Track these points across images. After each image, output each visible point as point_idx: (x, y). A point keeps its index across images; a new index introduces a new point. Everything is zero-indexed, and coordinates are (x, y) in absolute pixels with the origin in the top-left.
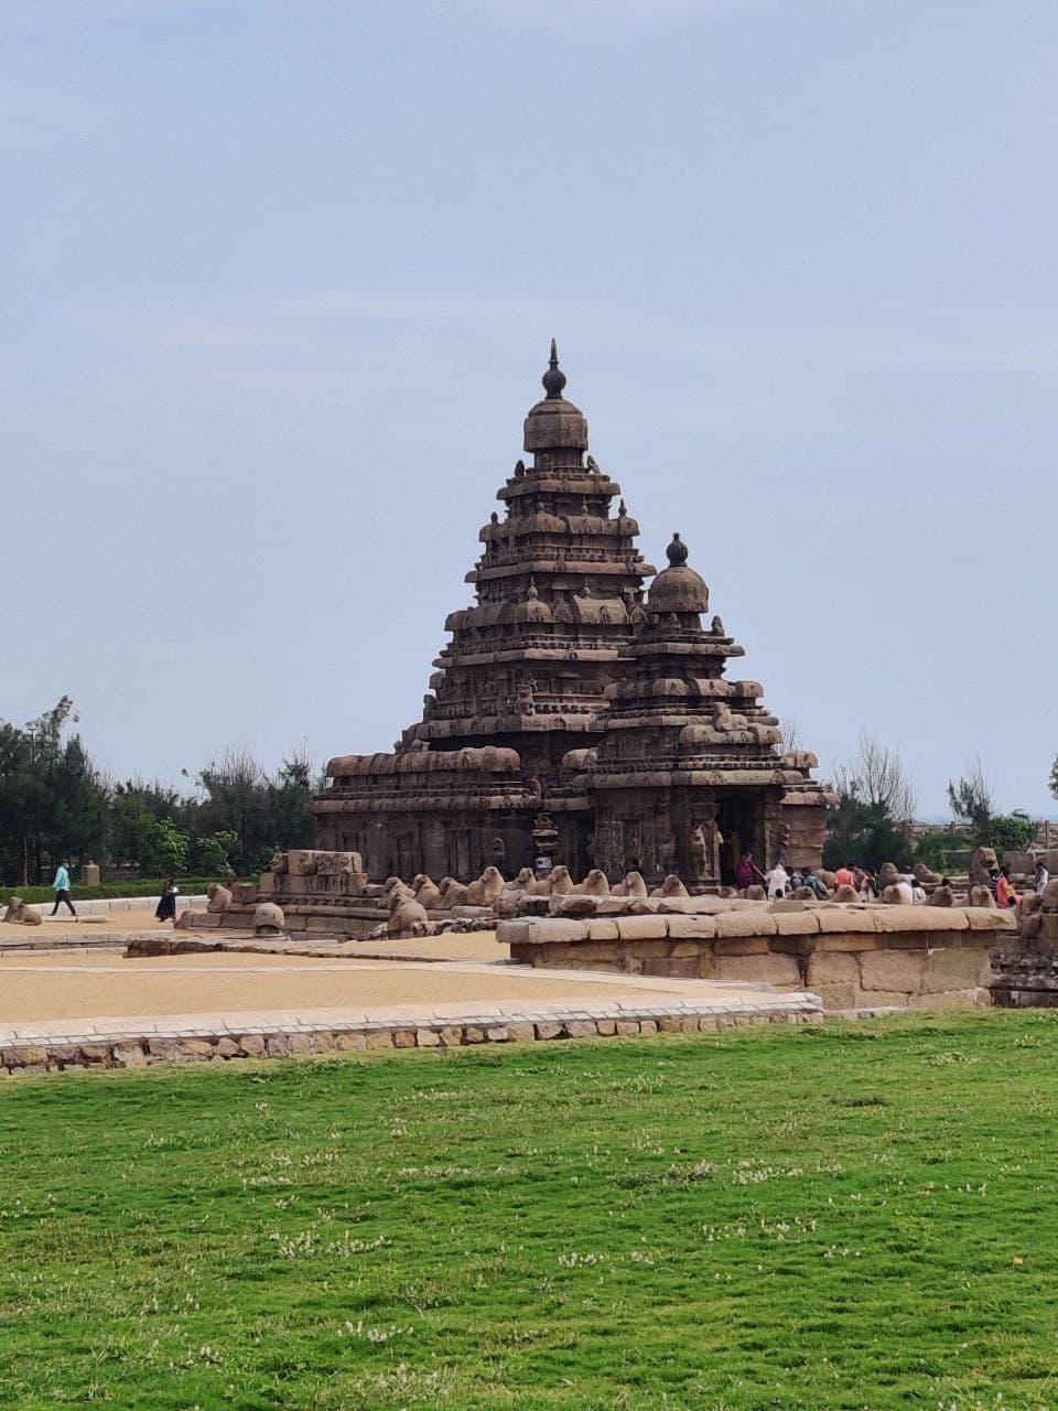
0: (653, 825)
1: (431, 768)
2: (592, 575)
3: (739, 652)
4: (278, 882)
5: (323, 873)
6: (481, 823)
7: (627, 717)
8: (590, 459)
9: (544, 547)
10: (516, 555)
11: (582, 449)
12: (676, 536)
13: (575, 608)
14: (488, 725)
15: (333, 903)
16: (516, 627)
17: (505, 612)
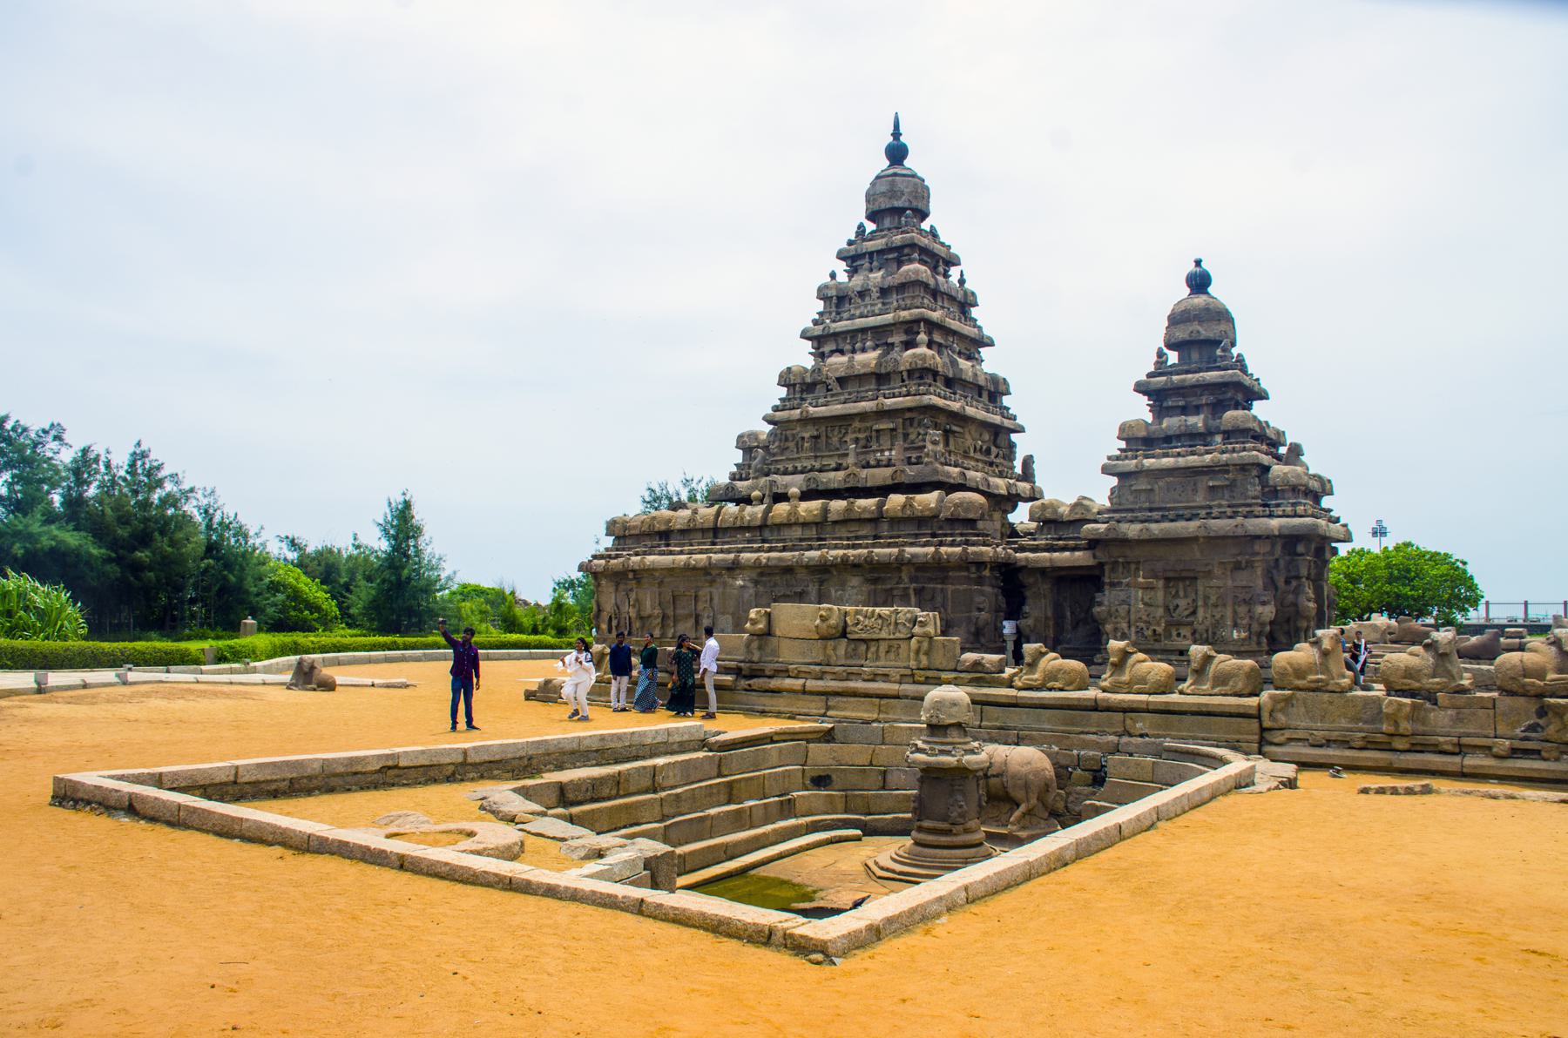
0: (1230, 583)
1: (832, 517)
2: (954, 333)
3: (1263, 396)
4: (755, 644)
5: (864, 636)
6: (944, 580)
7: (1179, 455)
8: (932, 226)
9: (923, 298)
10: (880, 305)
11: (923, 215)
12: (1198, 263)
13: (954, 363)
14: (881, 475)
15: (898, 677)
16: (905, 374)
17: (879, 364)
